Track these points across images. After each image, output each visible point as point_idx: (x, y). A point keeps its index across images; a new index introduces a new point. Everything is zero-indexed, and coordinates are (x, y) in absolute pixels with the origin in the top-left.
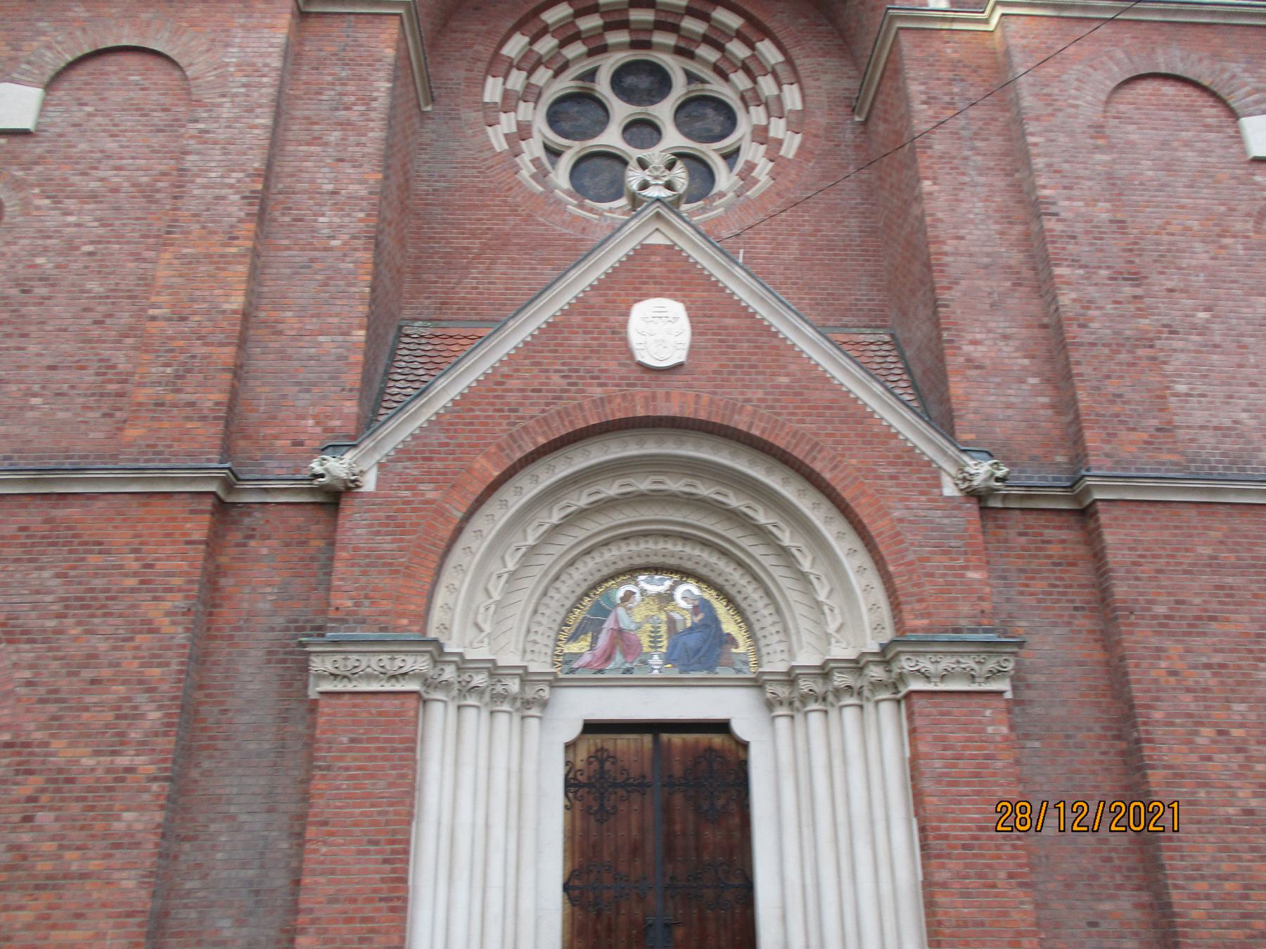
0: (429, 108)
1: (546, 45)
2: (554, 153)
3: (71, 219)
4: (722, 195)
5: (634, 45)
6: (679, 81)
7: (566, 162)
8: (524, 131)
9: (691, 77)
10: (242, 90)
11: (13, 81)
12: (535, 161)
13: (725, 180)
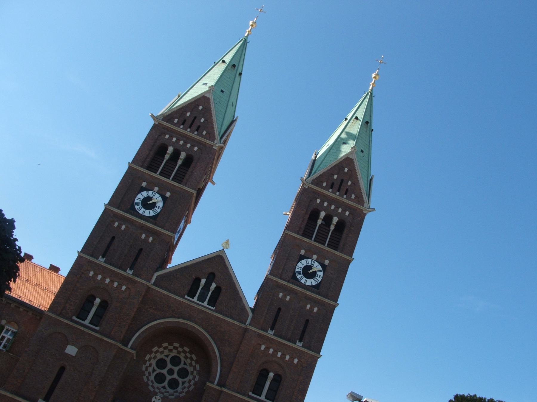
0: (135, 359)
1: (161, 349)
2: (154, 370)
3: (75, 374)
4: (177, 392)
5: (177, 353)
6: (182, 363)
7: (155, 373)
8: (150, 365)
9: (185, 364)
10: (105, 362)
11: (75, 346)
12: (149, 374)
13: (179, 389)
